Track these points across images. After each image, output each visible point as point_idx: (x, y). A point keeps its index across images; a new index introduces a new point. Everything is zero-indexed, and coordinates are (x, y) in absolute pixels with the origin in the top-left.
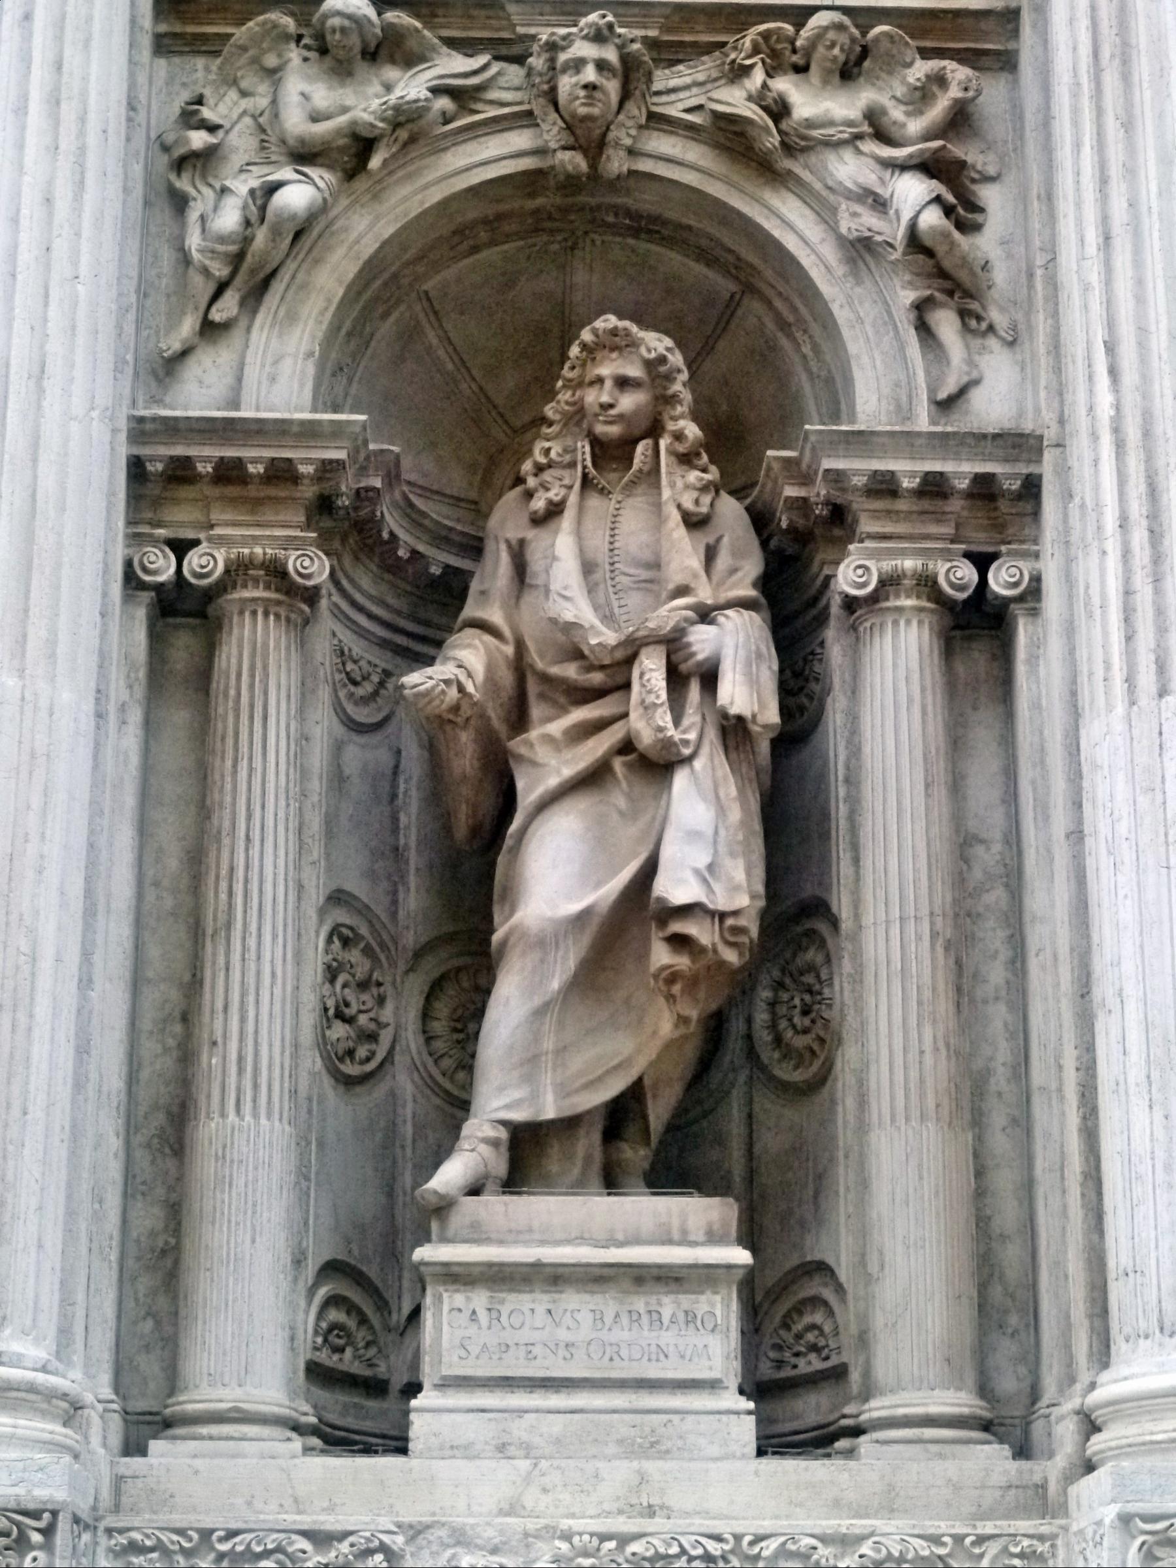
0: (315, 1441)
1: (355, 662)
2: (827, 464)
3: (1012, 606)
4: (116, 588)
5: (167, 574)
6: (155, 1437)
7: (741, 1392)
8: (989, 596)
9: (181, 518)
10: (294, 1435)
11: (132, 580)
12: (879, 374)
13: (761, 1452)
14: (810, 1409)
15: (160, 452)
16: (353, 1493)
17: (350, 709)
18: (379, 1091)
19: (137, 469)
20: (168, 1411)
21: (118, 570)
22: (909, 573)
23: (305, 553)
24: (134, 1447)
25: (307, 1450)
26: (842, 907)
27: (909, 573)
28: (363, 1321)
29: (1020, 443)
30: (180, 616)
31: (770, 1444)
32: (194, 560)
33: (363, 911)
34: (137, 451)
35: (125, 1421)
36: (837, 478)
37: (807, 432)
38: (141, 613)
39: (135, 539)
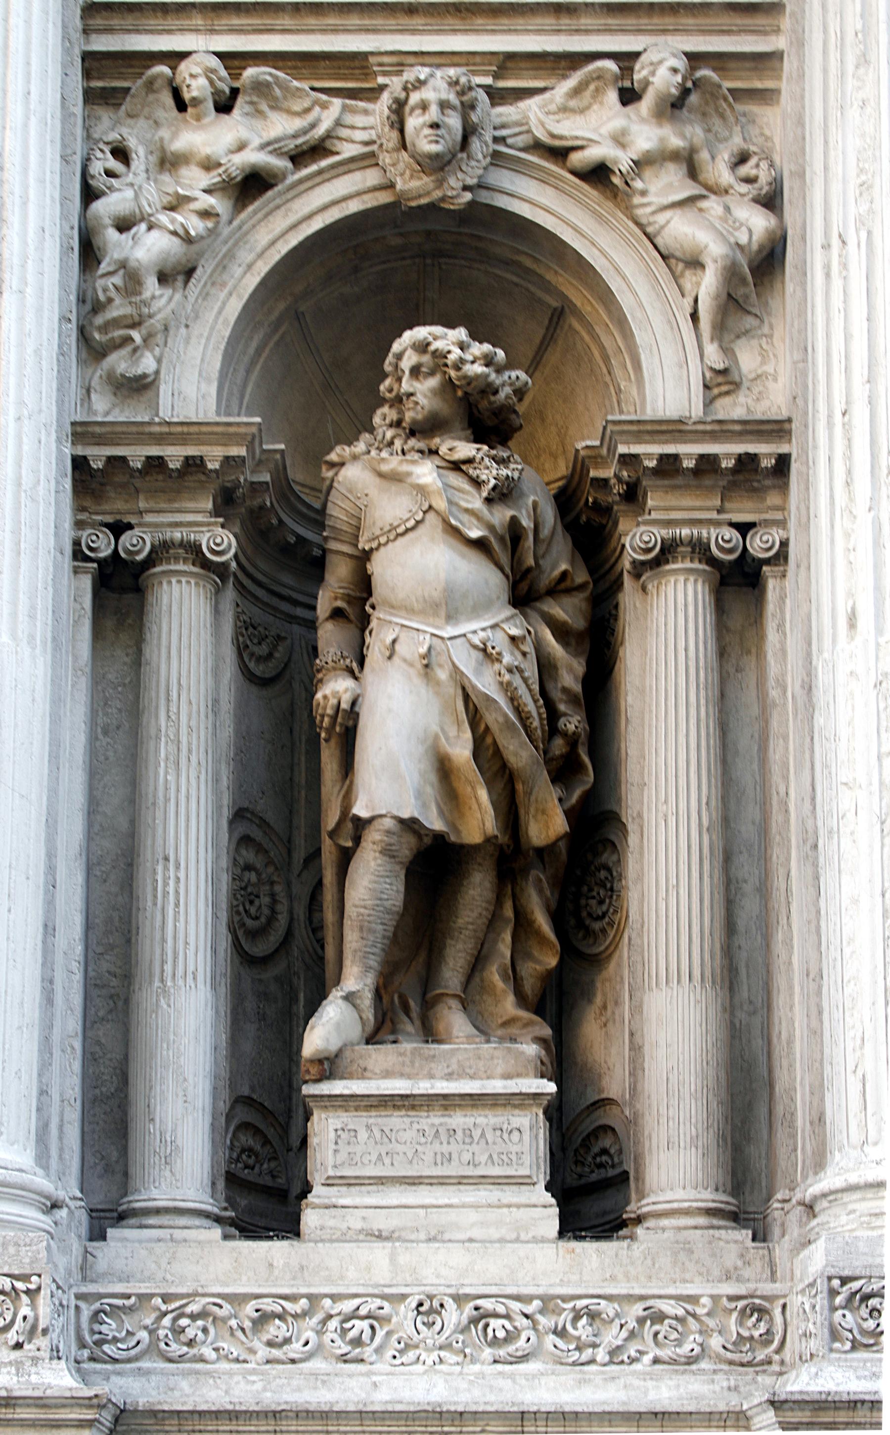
0: (233, 1231)
1: (255, 628)
2: (622, 449)
3: (765, 568)
4: (67, 561)
5: (105, 553)
6: (112, 1226)
7: (547, 1189)
8: (749, 560)
9: (116, 506)
10: (215, 1224)
11: (78, 554)
12: (664, 375)
13: (561, 1234)
14: (593, 1207)
15: (98, 455)
16: (260, 1265)
17: (252, 665)
18: (277, 969)
19: (79, 464)
20: (120, 1209)
21: (68, 549)
22: (685, 541)
23: (211, 552)
24: (98, 1234)
25: (226, 1237)
26: (628, 816)
27: (685, 541)
28: (266, 1142)
29: (778, 429)
30: (118, 589)
31: (572, 1226)
32: (127, 539)
33: (263, 824)
34: (80, 451)
35: (91, 1217)
36: (628, 460)
37: (607, 422)
38: (86, 582)
39: (79, 525)
